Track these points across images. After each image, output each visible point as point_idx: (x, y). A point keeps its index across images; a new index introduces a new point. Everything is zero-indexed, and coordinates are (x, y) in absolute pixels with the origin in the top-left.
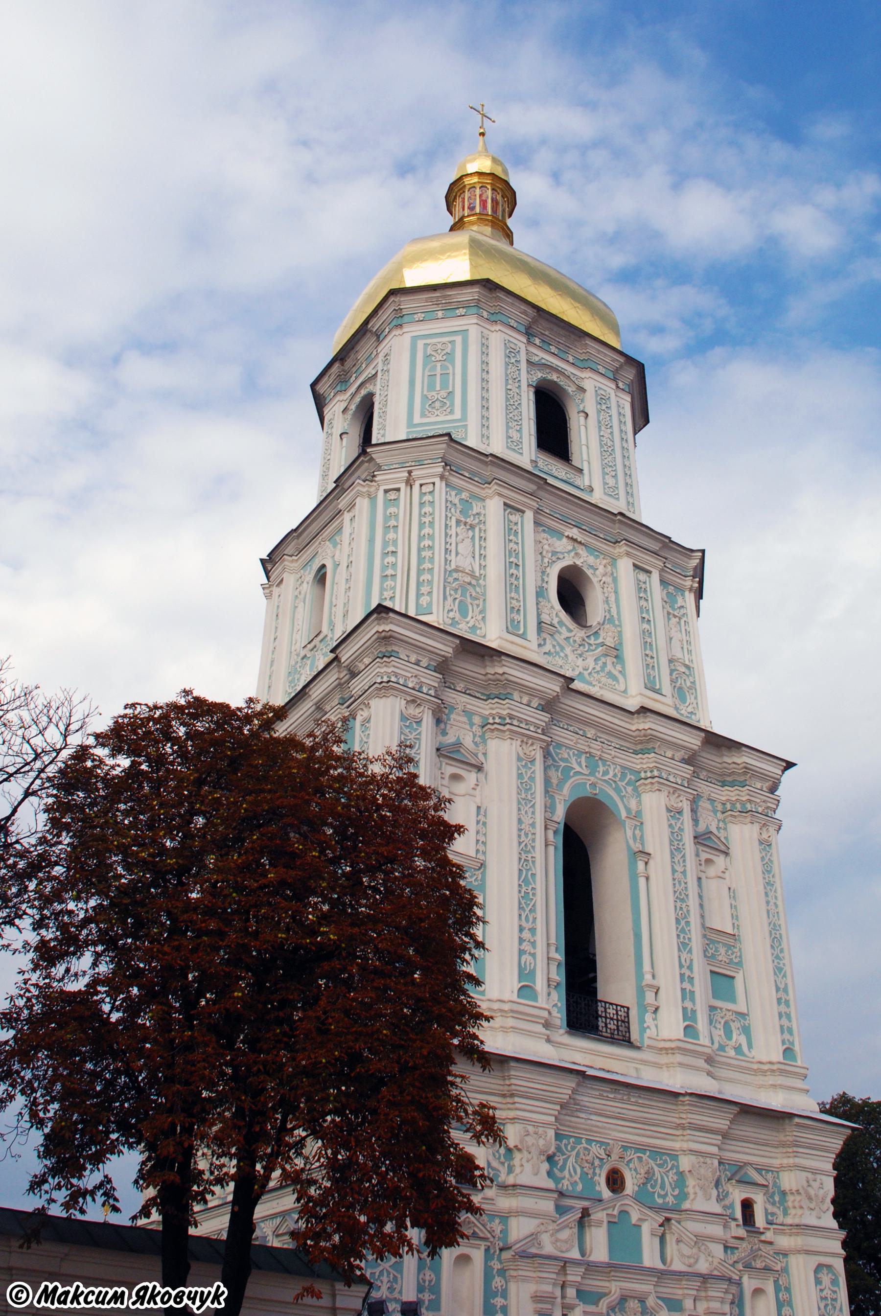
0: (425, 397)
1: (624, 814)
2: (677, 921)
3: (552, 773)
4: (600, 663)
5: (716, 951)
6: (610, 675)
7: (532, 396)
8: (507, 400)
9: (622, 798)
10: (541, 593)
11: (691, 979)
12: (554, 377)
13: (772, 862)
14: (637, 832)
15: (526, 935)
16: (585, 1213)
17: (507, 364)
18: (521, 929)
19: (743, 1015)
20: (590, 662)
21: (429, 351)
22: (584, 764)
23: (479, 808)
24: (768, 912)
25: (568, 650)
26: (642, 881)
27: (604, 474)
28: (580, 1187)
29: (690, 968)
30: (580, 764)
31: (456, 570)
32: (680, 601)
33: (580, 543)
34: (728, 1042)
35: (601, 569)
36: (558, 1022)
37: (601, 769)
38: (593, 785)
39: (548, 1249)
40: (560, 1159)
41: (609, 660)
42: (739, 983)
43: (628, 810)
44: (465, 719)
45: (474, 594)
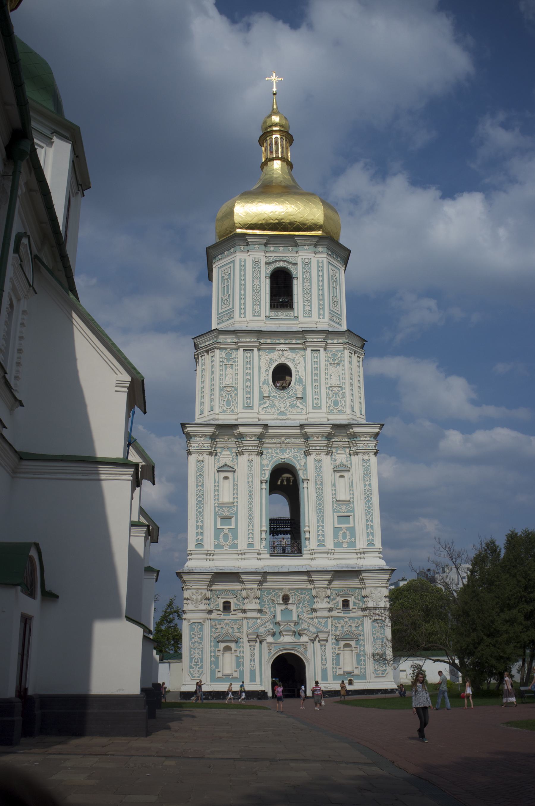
0: (222, 300)
7: (268, 281)
8: (253, 291)
9: (298, 461)
12: (281, 264)
14: (305, 472)
17: (253, 272)
21: (223, 275)
27: (304, 305)
35: (297, 358)
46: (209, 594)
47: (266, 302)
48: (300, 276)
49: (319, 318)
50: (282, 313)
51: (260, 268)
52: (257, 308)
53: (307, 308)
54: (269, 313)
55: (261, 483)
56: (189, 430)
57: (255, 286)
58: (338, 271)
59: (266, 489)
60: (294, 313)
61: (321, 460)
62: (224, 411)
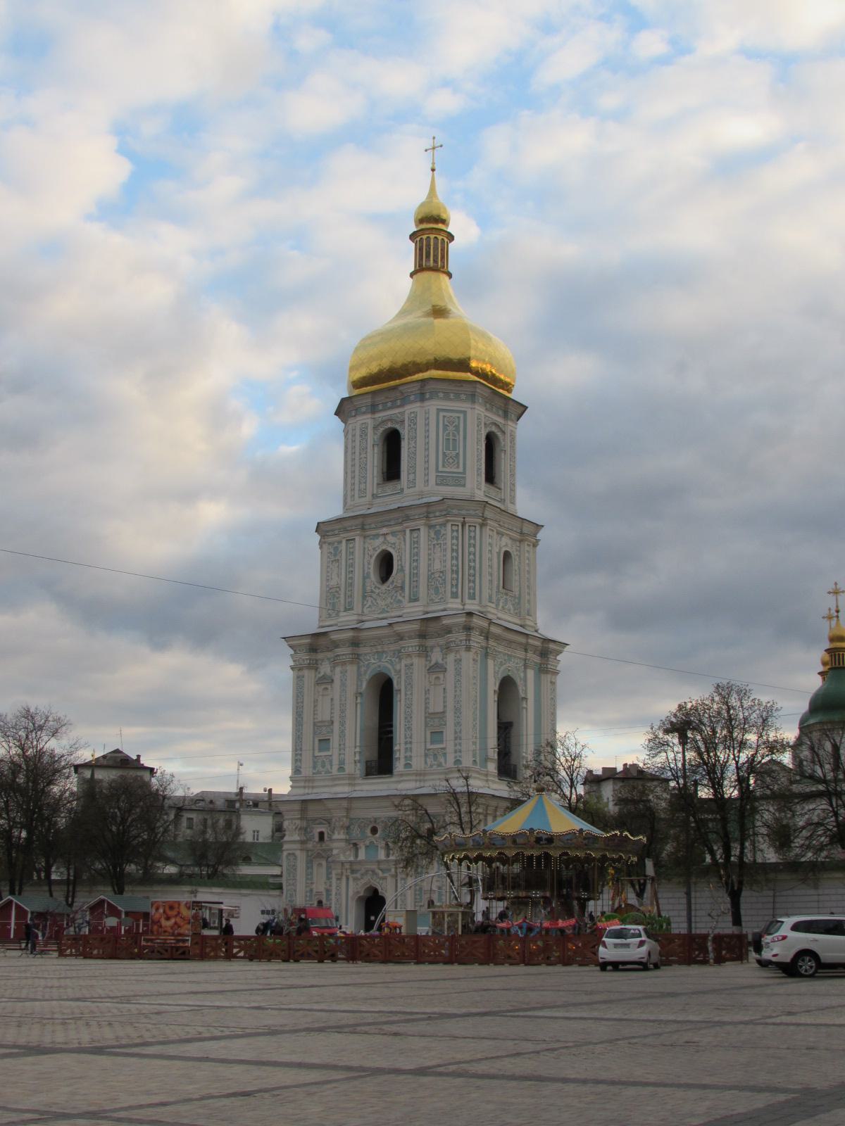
1: (392, 671)
2: (406, 718)
3: (363, 669)
4: (394, 598)
5: (434, 722)
6: (400, 601)
10: (365, 577)
11: (411, 743)
12: (389, 425)
13: (461, 668)
15: (342, 746)
16: (355, 845)
18: (340, 745)
19: (444, 749)
20: (389, 600)
22: (376, 657)
23: (332, 699)
24: (455, 696)
25: (379, 601)
26: (399, 703)
27: (409, 474)
28: (359, 835)
29: (411, 738)
30: (374, 659)
31: (331, 589)
32: (443, 532)
33: (387, 534)
34: (433, 762)
36: (359, 776)
37: (385, 656)
38: (379, 666)
39: (342, 858)
40: (352, 827)
41: (398, 594)
42: (444, 733)
43: (395, 671)
44: (327, 662)
45: (338, 596)
46: (304, 824)
47: (373, 477)
48: (406, 437)
49: (425, 486)
50: (390, 487)
51: (366, 435)
52: (363, 486)
53: (411, 477)
54: (377, 488)
55: (357, 698)
56: (289, 643)
57: (361, 460)
58: (461, 416)
59: (361, 703)
60: (400, 484)
61: (412, 665)
62: (330, 616)
